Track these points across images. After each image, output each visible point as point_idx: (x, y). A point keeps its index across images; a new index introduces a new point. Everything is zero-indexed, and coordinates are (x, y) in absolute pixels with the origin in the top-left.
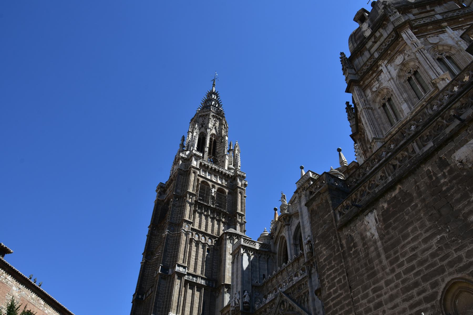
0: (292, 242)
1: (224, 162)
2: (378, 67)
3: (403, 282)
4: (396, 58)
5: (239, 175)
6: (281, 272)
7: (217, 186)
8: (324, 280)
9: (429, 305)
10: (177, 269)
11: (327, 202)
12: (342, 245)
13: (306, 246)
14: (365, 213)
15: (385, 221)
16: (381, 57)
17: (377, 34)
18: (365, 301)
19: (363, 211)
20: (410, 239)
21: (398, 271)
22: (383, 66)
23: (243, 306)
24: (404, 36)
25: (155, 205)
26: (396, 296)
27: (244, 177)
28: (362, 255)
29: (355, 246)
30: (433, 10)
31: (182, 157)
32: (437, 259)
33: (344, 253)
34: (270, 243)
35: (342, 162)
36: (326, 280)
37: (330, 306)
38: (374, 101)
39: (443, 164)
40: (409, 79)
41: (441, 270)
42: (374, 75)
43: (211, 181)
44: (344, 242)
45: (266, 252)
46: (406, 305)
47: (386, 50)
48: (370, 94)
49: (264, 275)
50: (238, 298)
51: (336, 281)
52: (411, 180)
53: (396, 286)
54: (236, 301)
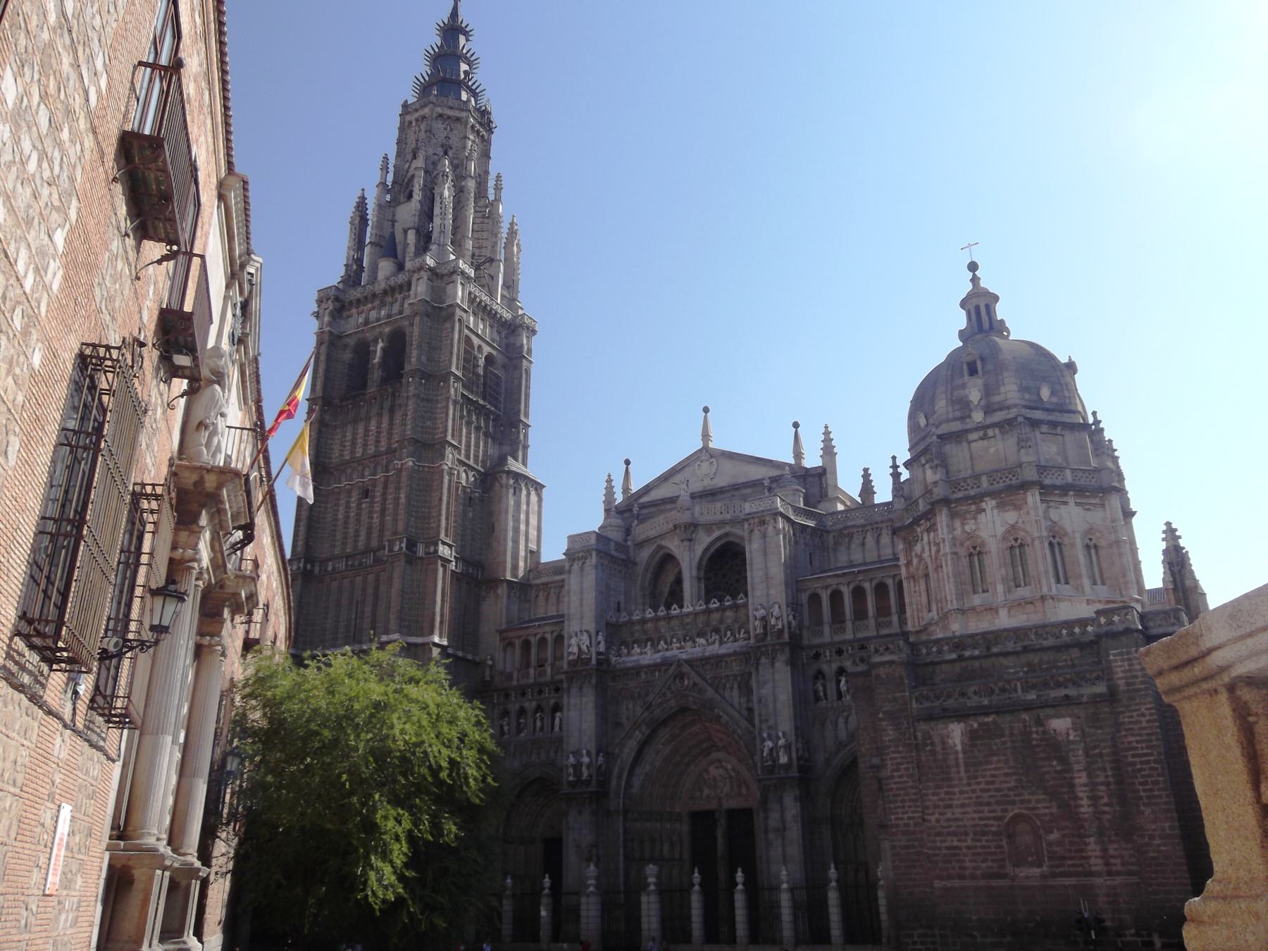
0: (694, 573)
1: (493, 278)
3: (978, 797)
7: (487, 349)
10: (444, 551)
11: (901, 677)
13: (757, 623)
15: (972, 739)
17: (990, 432)
22: (989, 504)
23: (598, 660)
24: (1030, 499)
25: (320, 343)
26: (969, 805)
27: (534, 332)
28: (940, 757)
29: (932, 744)
31: (430, 269)
32: (1011, 793)
33: (917, 745)
34: (626, 541)
35: (798, 454)
36: (889, 762)
37: (892, 789)
38: (962, 544)
39: (1039, 722)
40: (1012, 547)
41: (1013, 803)
42: (973, 507)
43: (477, 335)
44: (919, 735)
45: (623, 560)
46: (976, 816)
47: (1000, 492)
49: (619, 603)
52: (1008, 717)
53: (970, 798)
54: (584, 648)
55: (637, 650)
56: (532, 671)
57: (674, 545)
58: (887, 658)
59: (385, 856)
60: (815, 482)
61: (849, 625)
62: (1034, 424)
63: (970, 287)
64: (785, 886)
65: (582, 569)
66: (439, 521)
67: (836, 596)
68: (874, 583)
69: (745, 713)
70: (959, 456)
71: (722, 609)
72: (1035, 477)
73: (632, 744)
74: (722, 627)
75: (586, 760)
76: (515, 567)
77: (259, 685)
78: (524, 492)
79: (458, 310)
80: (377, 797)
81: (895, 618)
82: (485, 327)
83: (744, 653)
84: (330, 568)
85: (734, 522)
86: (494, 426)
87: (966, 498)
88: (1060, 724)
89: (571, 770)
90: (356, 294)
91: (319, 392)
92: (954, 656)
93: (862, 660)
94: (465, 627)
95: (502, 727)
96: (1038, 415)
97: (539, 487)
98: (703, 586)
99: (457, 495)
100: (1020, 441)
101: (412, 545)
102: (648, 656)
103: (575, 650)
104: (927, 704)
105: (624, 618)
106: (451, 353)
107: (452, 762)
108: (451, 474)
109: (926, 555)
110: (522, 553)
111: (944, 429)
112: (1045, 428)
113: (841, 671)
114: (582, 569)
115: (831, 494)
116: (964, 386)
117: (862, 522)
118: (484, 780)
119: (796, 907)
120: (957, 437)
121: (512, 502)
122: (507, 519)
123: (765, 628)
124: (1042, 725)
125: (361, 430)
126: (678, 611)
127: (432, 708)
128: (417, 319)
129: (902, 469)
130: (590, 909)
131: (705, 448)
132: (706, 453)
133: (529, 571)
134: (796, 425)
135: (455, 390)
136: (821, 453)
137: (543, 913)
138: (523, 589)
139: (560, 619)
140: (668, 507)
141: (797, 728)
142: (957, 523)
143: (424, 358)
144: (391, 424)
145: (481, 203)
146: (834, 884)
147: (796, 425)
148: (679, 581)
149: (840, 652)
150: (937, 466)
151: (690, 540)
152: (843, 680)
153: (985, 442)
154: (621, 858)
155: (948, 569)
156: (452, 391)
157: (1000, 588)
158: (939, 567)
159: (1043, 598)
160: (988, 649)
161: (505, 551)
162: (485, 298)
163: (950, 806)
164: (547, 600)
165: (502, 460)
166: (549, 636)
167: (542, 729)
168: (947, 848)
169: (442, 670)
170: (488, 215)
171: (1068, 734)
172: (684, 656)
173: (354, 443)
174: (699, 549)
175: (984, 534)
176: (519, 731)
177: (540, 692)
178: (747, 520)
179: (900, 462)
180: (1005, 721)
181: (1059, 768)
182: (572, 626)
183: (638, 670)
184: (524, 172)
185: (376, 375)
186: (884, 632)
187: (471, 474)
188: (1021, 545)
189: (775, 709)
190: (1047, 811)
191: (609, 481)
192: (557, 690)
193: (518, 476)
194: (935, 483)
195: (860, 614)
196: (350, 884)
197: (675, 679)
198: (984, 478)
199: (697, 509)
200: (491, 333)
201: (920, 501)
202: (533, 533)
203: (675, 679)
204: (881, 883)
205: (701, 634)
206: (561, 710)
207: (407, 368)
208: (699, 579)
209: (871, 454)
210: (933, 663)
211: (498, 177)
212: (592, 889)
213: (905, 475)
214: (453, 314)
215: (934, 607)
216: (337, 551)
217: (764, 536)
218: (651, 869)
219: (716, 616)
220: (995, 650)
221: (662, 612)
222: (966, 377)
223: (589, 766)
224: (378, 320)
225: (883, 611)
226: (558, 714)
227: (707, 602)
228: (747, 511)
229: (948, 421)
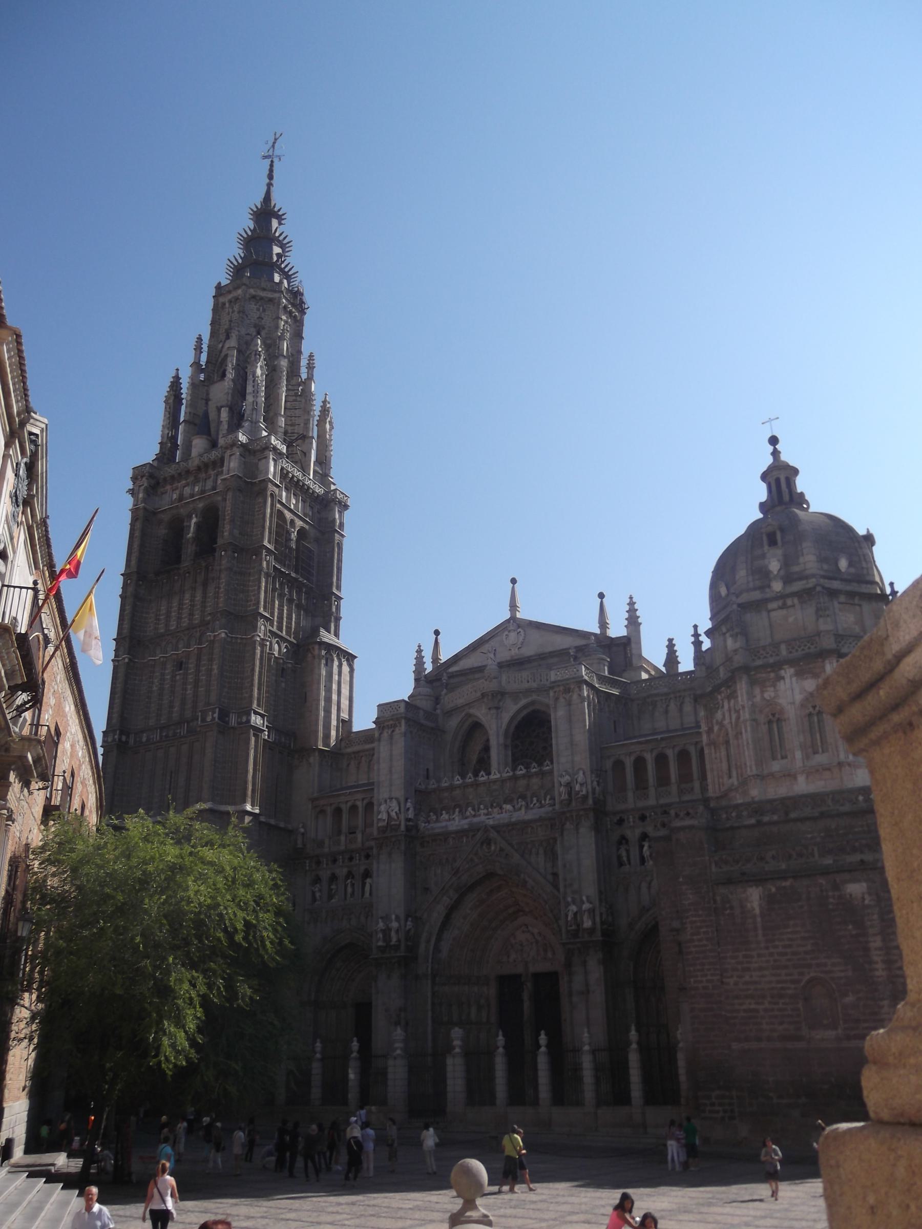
0: (501, 740)
1: (306, 454)
2: (781, 669)
3: (775, 961)
4: (806, 678)
5: (340, 502)
7: (299, 523)
9: (793, 986)
10: (256, 720)
13: (562, 789)
16: (791, 662)
17: (789, 602)
18: (733, 961)
20: (789, 930)
21: (772, 950)
22: (788, 672)
23: (406, 826)
27: (346, 507)
29: (732, 908)
30: (860, 605)
31: (242, 445)
34: (435, 709)
35: (603, 624)
39: (836, 887)
40: (810, 715)
42: (772, 675)
44: (718, 898)
48: (758, 698)
50: (397, 809)
51: (702, 930)
54: (393, 814)
55: (445, 816)
56: (343, 838)
57: (481, 713)
58: (688, 822)
59: (179, 1023)
60: (621, 651)
61: (652, 791)
62: (833, 593)
63: (770, 460)
64: (586, 1048)
65: (391, 737)
66: (252, 691)
67: (640, 763)
68: (677, 750)
69: (550, 877)
70: (759, 624)
71: (528, 776)
72: (834, 646)
73: (440, 911)
75: (395, 925)
76: (327, 736)
77: (58, 851)
78: (336, 663)
79: (270, 485)
80: (171, 959)
81: (697, 785)
82: (297, 501)
84: (144, 739)
86: (307, 599)
87: (764, 667)
88: (856, 889)
89: (380, 935)
90: (170, 470)
91: (134, 568)
92: (753, 821)
93: (664, 825)
94: (276, 796)
95: (314, 893)
96: (836, 585)
97: (350, 658)
98: (510, 753)
99: (269, 665)
100: (818, 610)
101: (224, 715)
102: (455, 822)
103: (384, 816)
105: (432, 785)
106: (264, 527)
107: (247, 924)
108: (263, 645)
109: (726, 722)
110: (334, 722)
111: (744, 598)
112: (842, 598)
113: (644, 837)
114: (391, 737)
115: (635, 662)
116: (763, 556)
117: (665, 690)
118: (281, 943)
119: (597, 1069)
120: (757, 606)
121: (324, 672)
122: (319, 689)
123: (570, 794)
125: (175, 604)
126: (485, 778)
127: (228, 870)
128: (230, 495)
129: (704, 638)
130: (397, 1074)
131: (513, 618)
132: (513, 624)
133: (339, 741)
134: (601, 596)
135: (267, 562)
136: (626, 623)
137: (352, 1076)
138: (334, 757)
139: (370, 787)
140: (477, 676)
141: (600, 892)
142: (757, 691)
143: (236, 532)
144: (205, 596)
145: (294, 382)
146: (634, 1046)
147: (601, 596)
148: (487, 749)
149: (643, 818)
150: (737, 635)
151: (497, 708)
152: (646, 845)
153: (784, 612)
154: (430, 1022)
155: (747, 735)
156: (265, 564)
157: (798, 755)
158: (738, 735)
159: (840, 765)
160: (787, 814)
161: (317, 720)
162: (298, 474)
163: (748, 969)
164: (358, 768)
165: (315, 632)
166: (359, 804)
167: (353, 894)
168: (745, 1011)
169: (240, 834)
170: (301, 396)
171: (863, 899)
172: (491, 822)
173: (168, 616)
174: (506, 717)
175: (782, 701)
176: (330, 897)
177: (351, 859)
178: (552, 688)
179: (701, 631)
181: (854, 932)
182: (382, 793)
183: (445, 836)
184: (338, 353)
185: (189, 550)
186: (686, 798)
187: (283, 645)
188: (820, 713)
190: (842, 974)
191: (419, 651)
192: (368, 856)
193: (330, 648)
194: (735, 651)
195: (663, 780)
196: (143, 1049)
197: (482, 844)
198: (783, 647)
199: (504, 678)
200: (304, 508)
201: (721, 670)
202: (345, 703)
203: (482, 844)
204: (681, 1045)
205: (508, 801)
206: (371, 877)
207: (220, 542)
208: (506, 746)
209: (674, 623)
210: (732, 828)
211: (311, 356)
212: (399, 1052)
213: (707, 644)
214: (265, 489)
215: (734, 774)
216: (152, 722)
217: (569, 704)
218: (457, 1033)
219: (522, 783)
220: (793, 815)
221: (470, 778)
222: (766, 547)
223: (397, 931)
224: (192, 496)
225: (685, 777)
226: (368, 881)
227: (514, 770)
228: (553, 679)
229: (748, 590)
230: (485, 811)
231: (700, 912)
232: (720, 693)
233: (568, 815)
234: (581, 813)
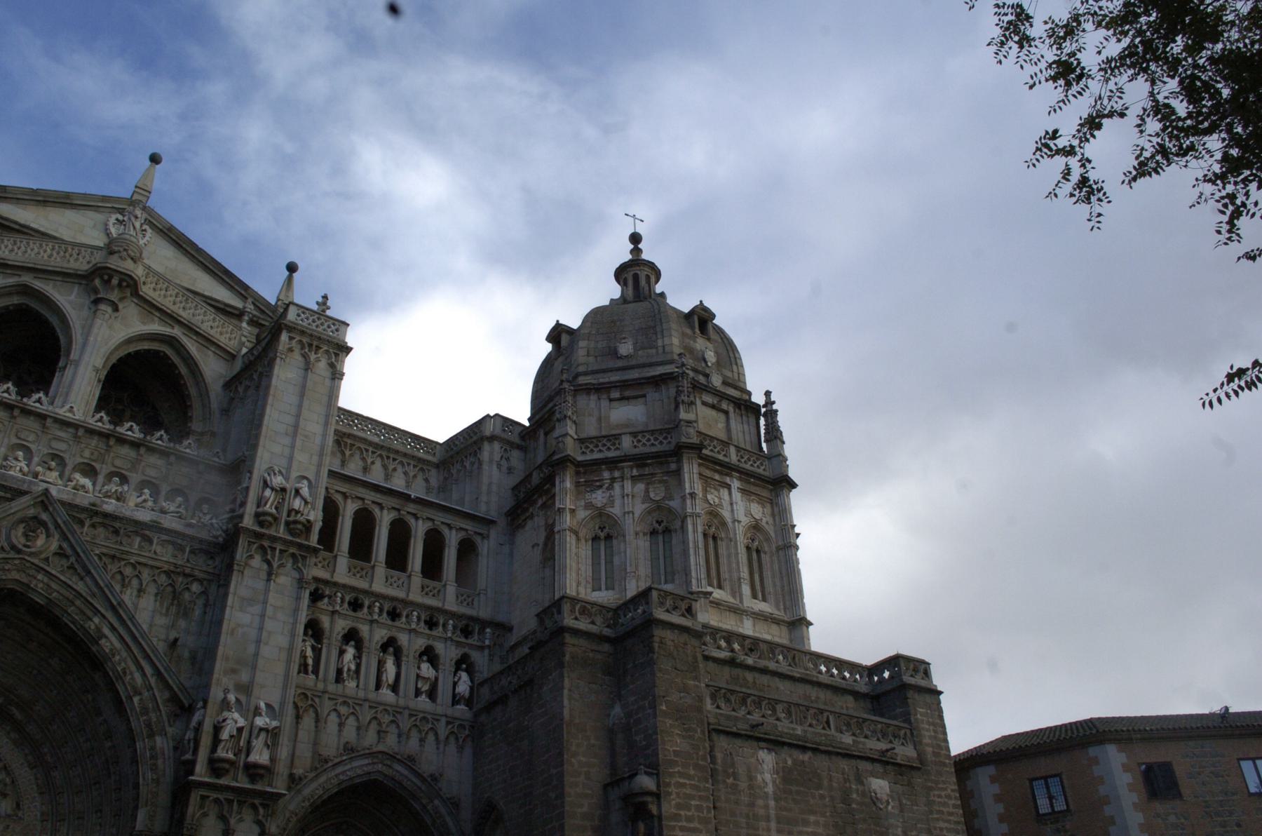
2: (727, 475)
6: (27, 412)
8: (668, 785)
11: (695, 657)
12: (713, 758)
14: (762, 744)
15: (786, 780)
16: (745, 475)
19: (759, 739)
36: (672, 789)
42: (717, 477)
44: (719, 756)
51: (693, 803)
68: (429, 525)
74: (135, 478)
83: (192, 538)
85: (189, 328)
104: (725, 710)
123: (276, 508)
124: (862, 783)
151: (116, 309)
171: (888, 803)
180: (822, 763)
189: (256, 655)
205: (90, 471)
217: (308, 367)
219: (125, 451)
230: (26, 469)
231: (692, 772)
232: (611, 470)
233: (266, 544)
234: (292, 550)
